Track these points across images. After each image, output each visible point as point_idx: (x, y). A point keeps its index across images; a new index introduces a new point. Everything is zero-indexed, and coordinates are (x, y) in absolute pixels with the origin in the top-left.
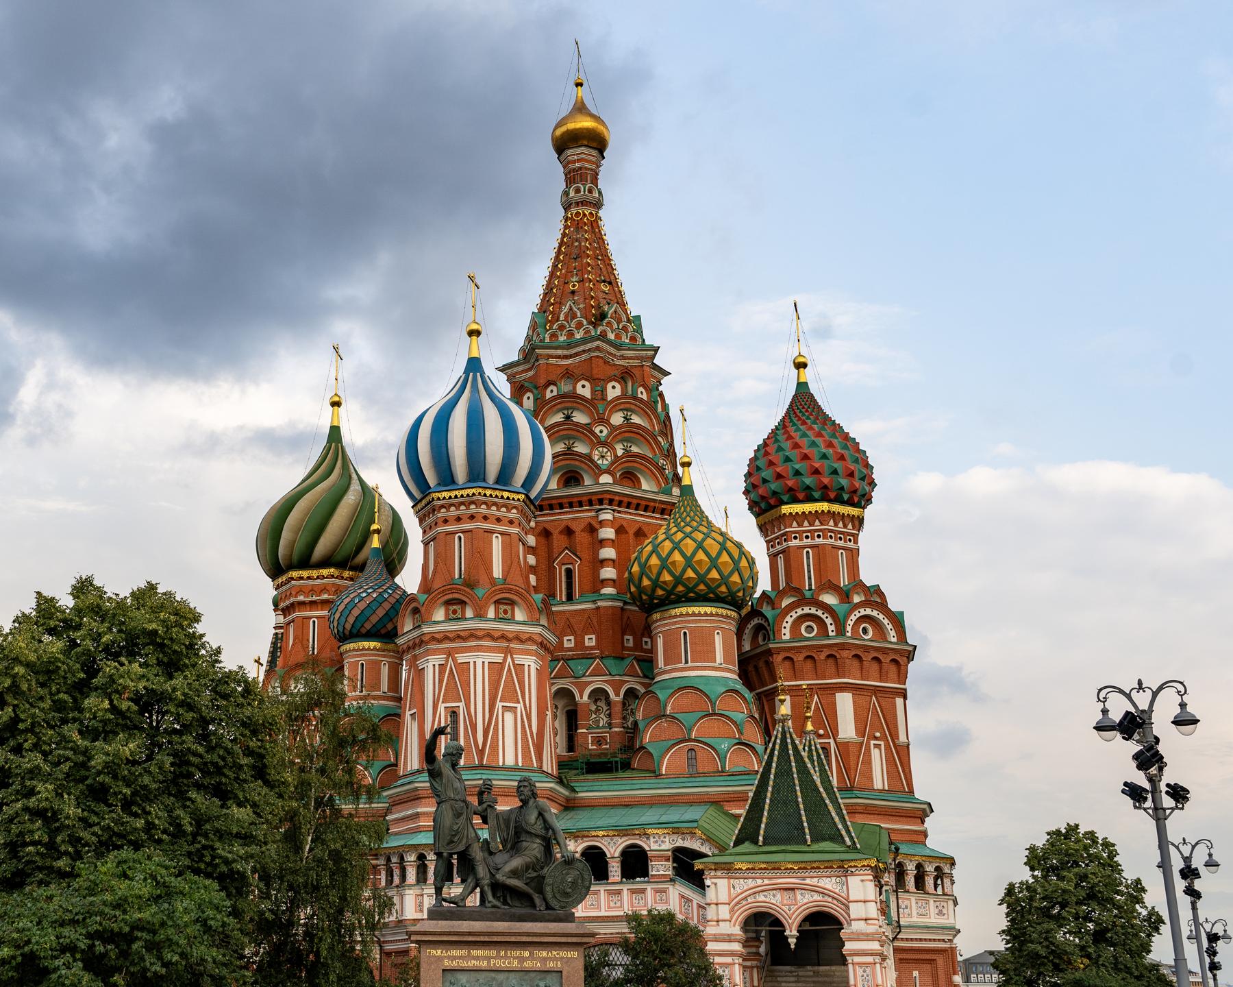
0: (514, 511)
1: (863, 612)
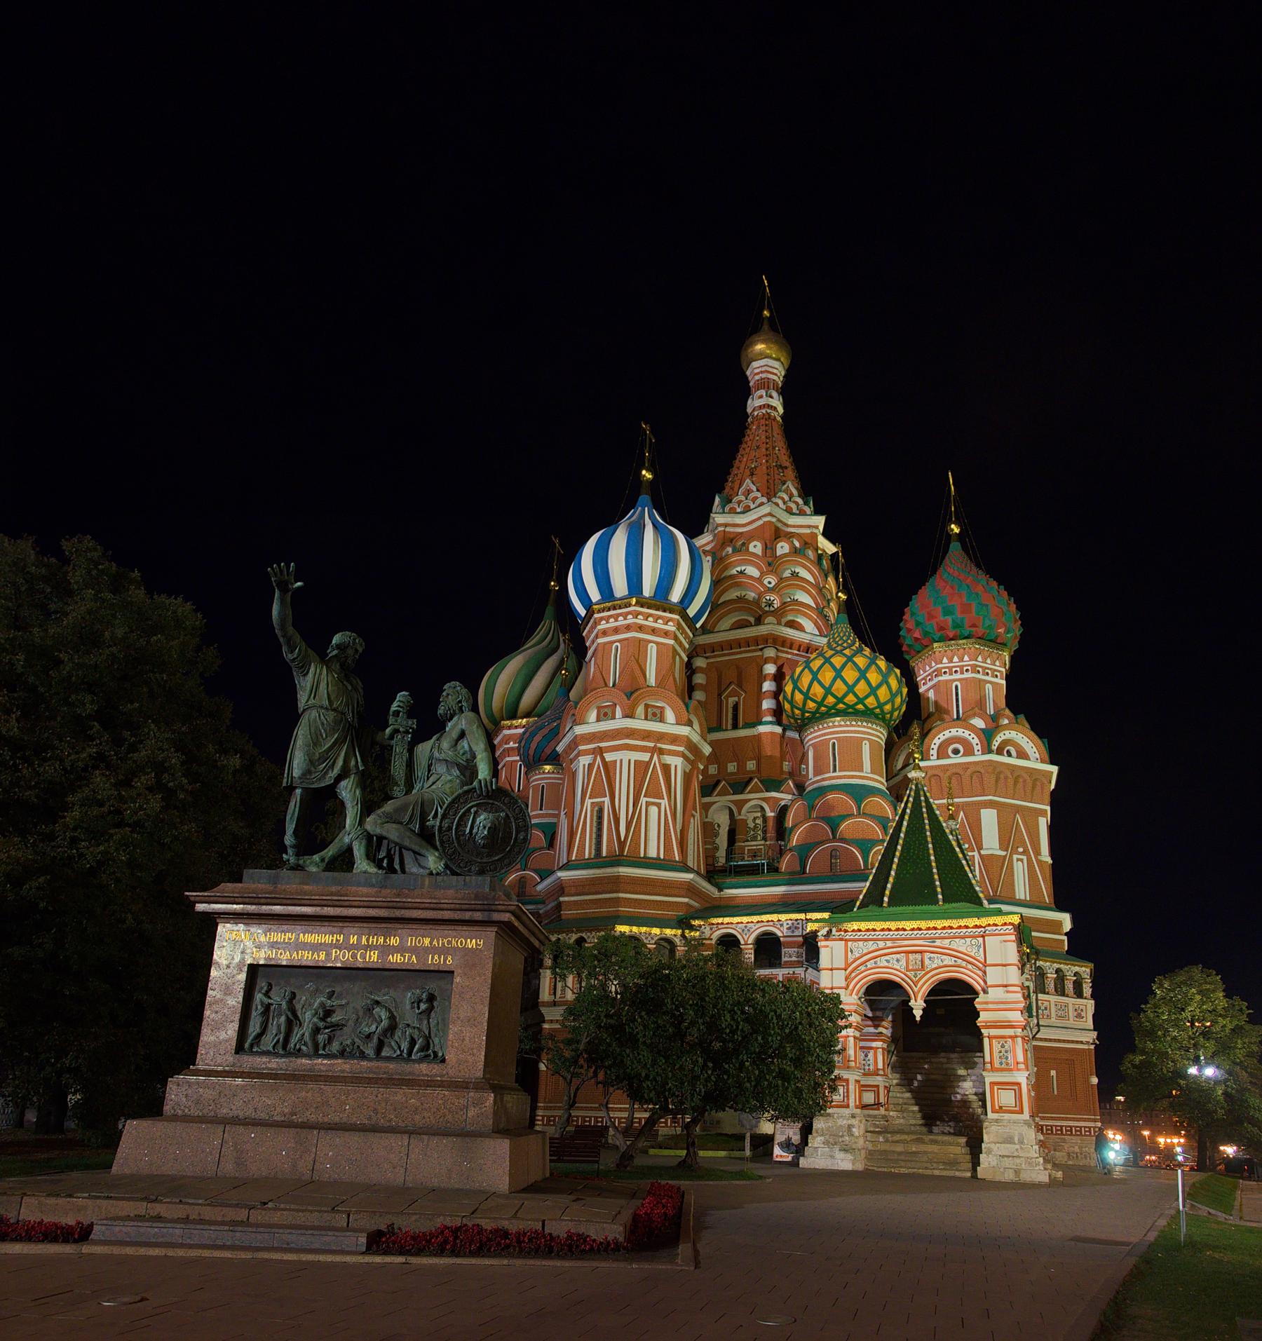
0: (671, 623)
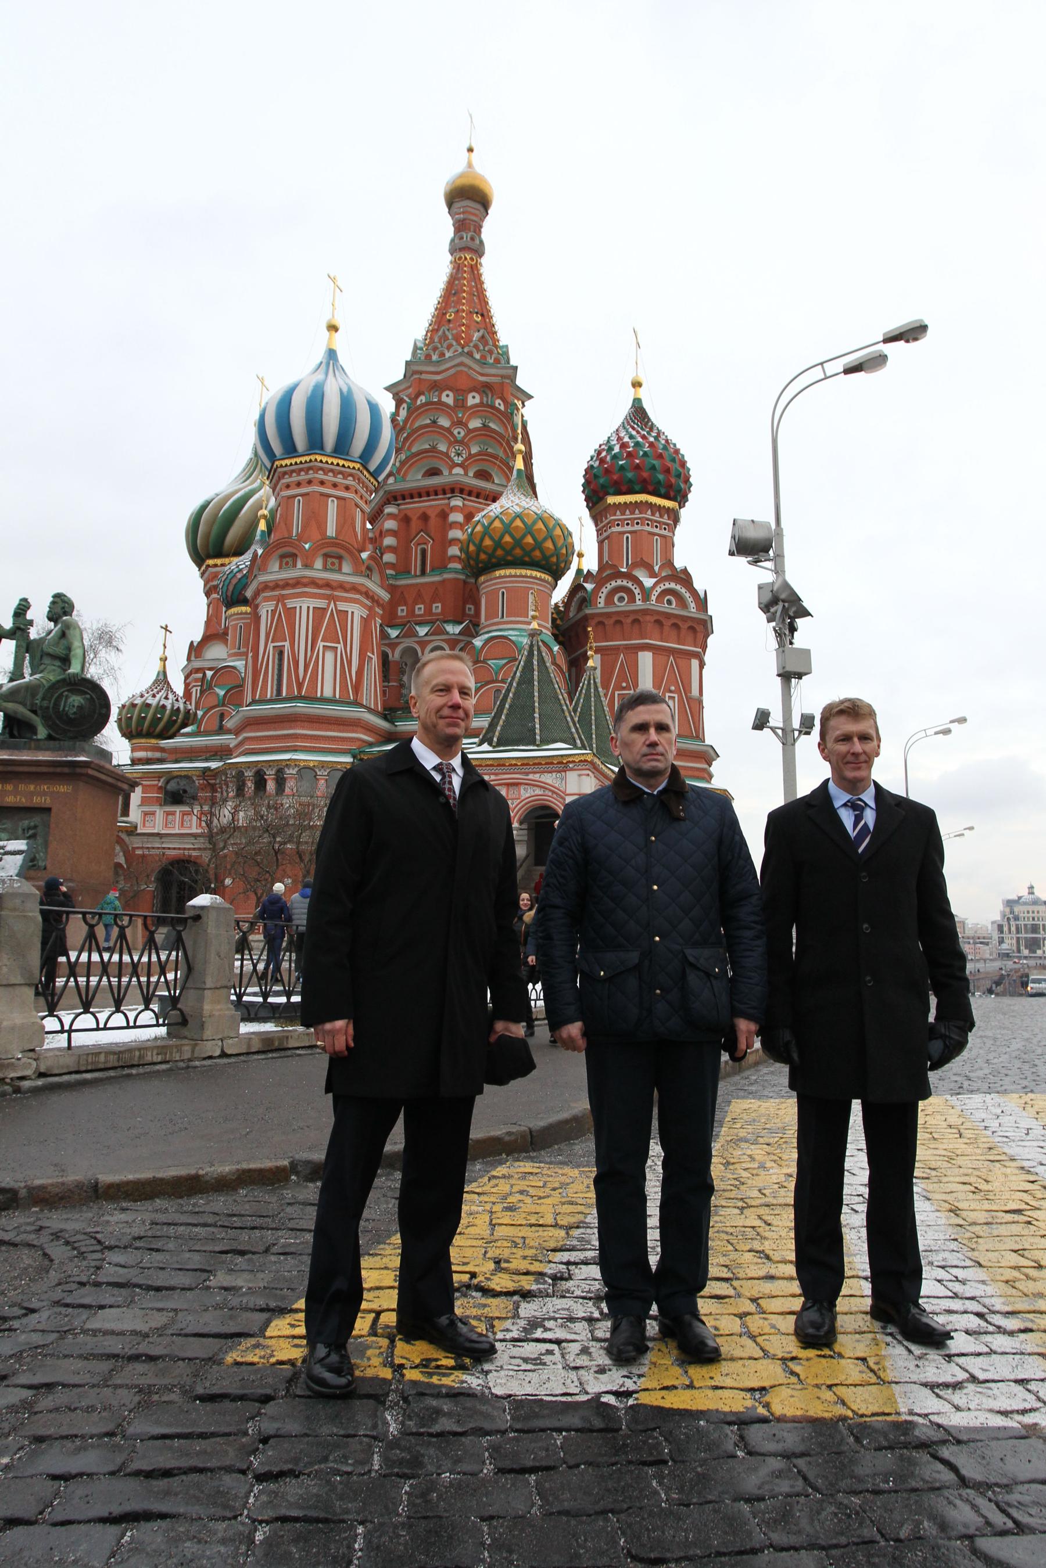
0: (350, 478)
1: (667, 585)
